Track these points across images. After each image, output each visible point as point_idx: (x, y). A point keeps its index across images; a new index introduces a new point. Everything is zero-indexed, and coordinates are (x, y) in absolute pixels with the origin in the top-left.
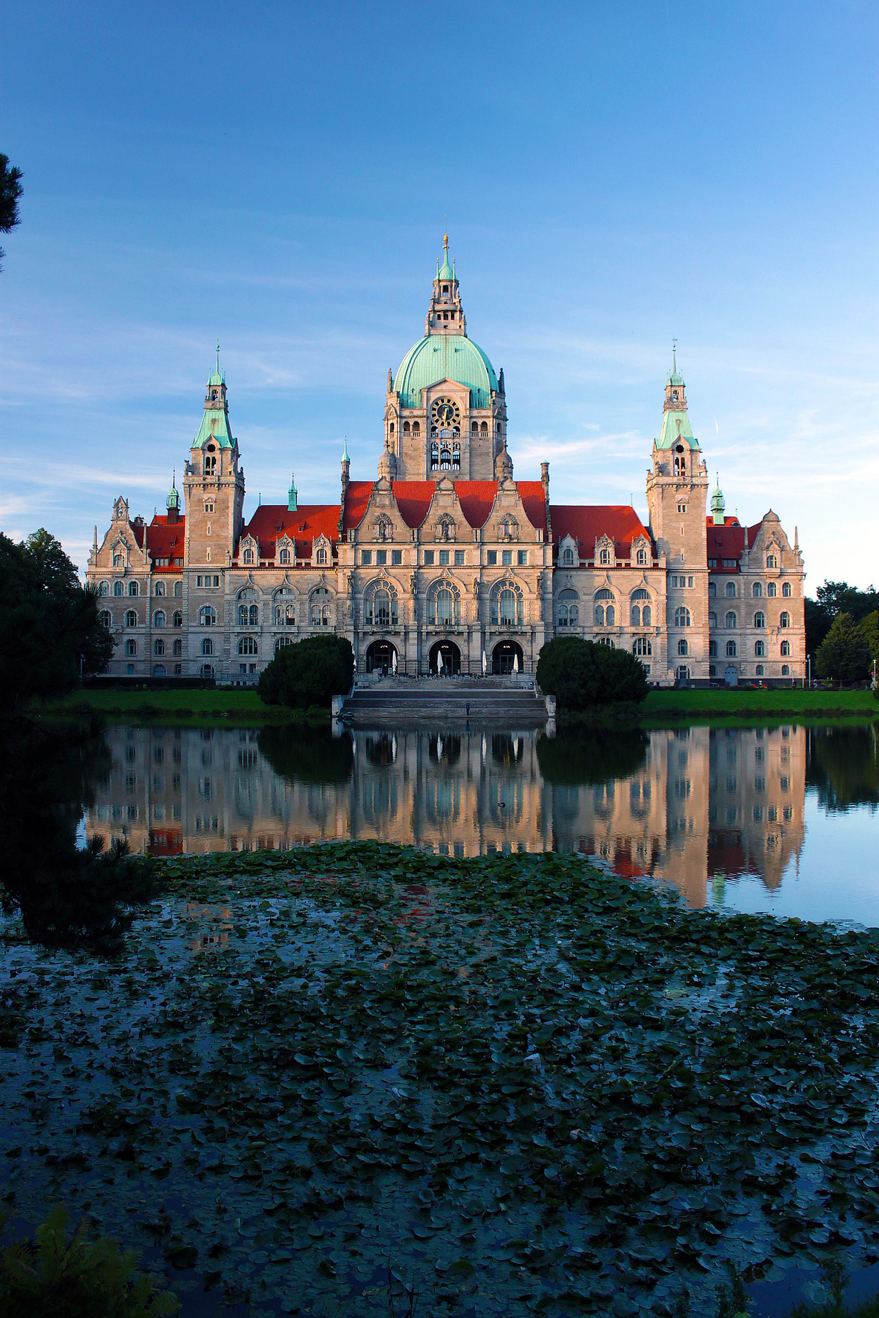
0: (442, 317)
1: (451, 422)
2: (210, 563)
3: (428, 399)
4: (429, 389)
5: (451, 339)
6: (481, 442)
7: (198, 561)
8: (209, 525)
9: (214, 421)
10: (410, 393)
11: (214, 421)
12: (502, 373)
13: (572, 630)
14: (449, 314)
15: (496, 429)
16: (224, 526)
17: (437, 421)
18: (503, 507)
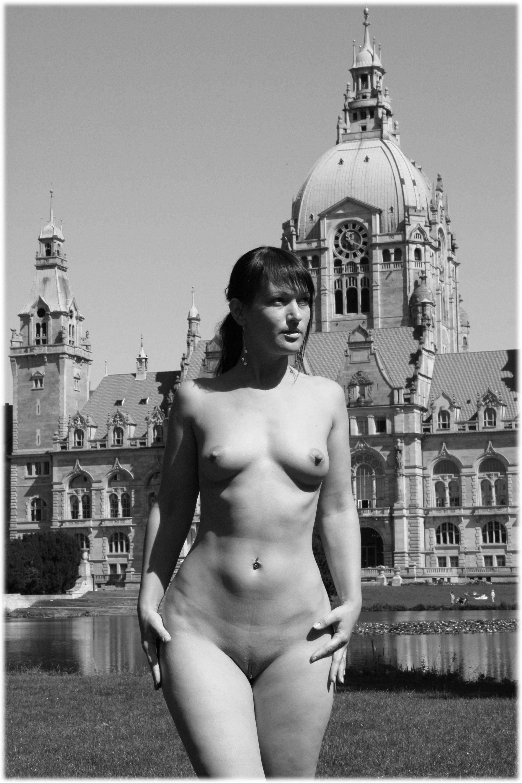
0: (359, 116)
1: (359, 253)
2: (40, 447)
3: (329, 226)
4: (330, 213)
5: (367, 144)
6: (393, 275)
7: (27, 446)
8: (38, 402)
9: (45, 281)
10: (309, 220)
11: (45, 281)
12: (439, 179)
13: (449, 513)
14: (368, 112)
15: (411, 256)
16: (55, 403)
17: (341, 252)
18: (354, 363)
